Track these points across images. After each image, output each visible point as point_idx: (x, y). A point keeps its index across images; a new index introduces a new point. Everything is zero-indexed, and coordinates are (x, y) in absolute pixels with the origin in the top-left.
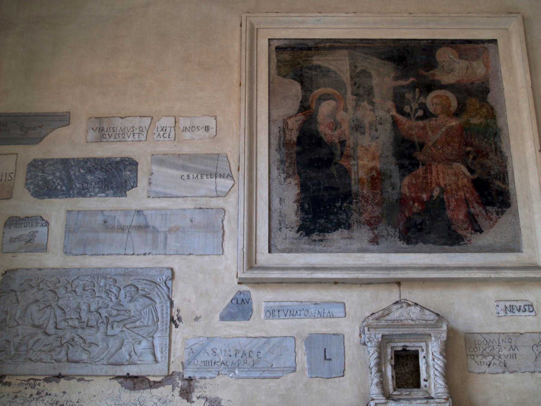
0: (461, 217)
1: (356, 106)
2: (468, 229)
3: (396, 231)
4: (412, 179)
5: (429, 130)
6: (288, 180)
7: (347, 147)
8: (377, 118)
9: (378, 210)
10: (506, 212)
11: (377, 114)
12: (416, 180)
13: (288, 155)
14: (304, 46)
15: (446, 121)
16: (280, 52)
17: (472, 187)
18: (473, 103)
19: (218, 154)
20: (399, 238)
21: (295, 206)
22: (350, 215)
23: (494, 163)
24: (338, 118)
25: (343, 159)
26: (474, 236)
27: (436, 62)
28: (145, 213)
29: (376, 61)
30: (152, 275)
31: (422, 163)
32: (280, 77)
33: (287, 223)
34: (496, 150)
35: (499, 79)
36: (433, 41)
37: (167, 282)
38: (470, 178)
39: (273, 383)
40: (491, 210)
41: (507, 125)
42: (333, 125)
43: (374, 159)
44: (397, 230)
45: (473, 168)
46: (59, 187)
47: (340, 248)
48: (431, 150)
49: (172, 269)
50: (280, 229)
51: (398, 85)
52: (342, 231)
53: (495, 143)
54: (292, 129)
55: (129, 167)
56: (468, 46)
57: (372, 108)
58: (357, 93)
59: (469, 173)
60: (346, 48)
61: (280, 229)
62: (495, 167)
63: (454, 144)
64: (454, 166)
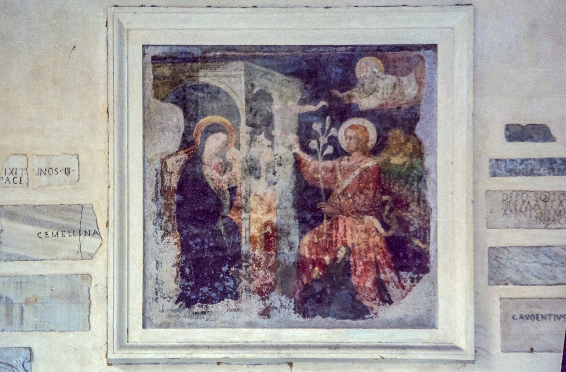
0: (369, 284)
1: (251, 141)
2: (375, 299)
3: (291, 302)
4: (313, 237)
5: (339, 173)
6: (167, 239)
7: (238, 195)
8: (277, 157)
9: (272, 276)
10: (423, 278)
11: (276, 152)
12: (318, 238)
13: (167, 207)
14: (188, 56)
15: (361, 161)
16: (157, 65)
17: (385, 247)
18: (397, 134)
19: (83, 206)
20: (294, 309)
21: (174, 271)
22: (238, 281)
23: (414, 217)
24: (229, 156)
25: (232, 212)
26: (382, 307)
27: (355, 79)
29: (279, 77)
30: (7, 357)
31: (327, 216)
32: (157, 101)
33: (164, 291)
34: (419, 200)
35: (433, 102)
36: (354, 48)
37: (25, 365)
38: (384, 235)
40: (404, 276)
42: (222, 166)
43: (269, 211)
44: (293, 300)
45: (388, 222)
47: (224, 322)
48: (340, 199)
49: (30, 349)
50: (157, 299)
51: (305, 111)
52: (228, 302)
53: (419, 190)
54: (172, 172)
56: (399, 54)
57: (270, 143)
58: (253, 123)
59: (382, 229)
60: (242, 59)
61: (157, 299)
62: (416, 221)
63: (368, 192)
64: (366, 220)
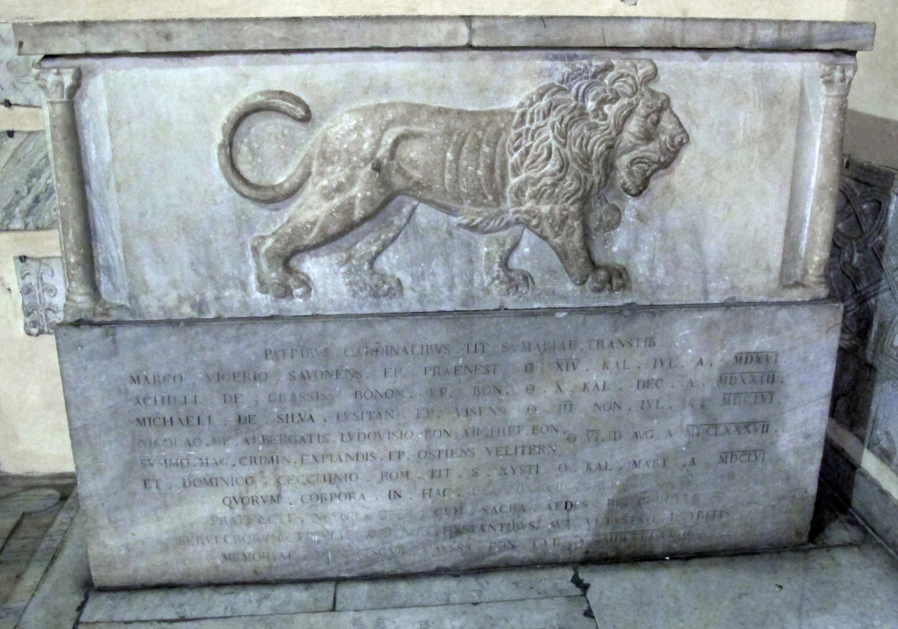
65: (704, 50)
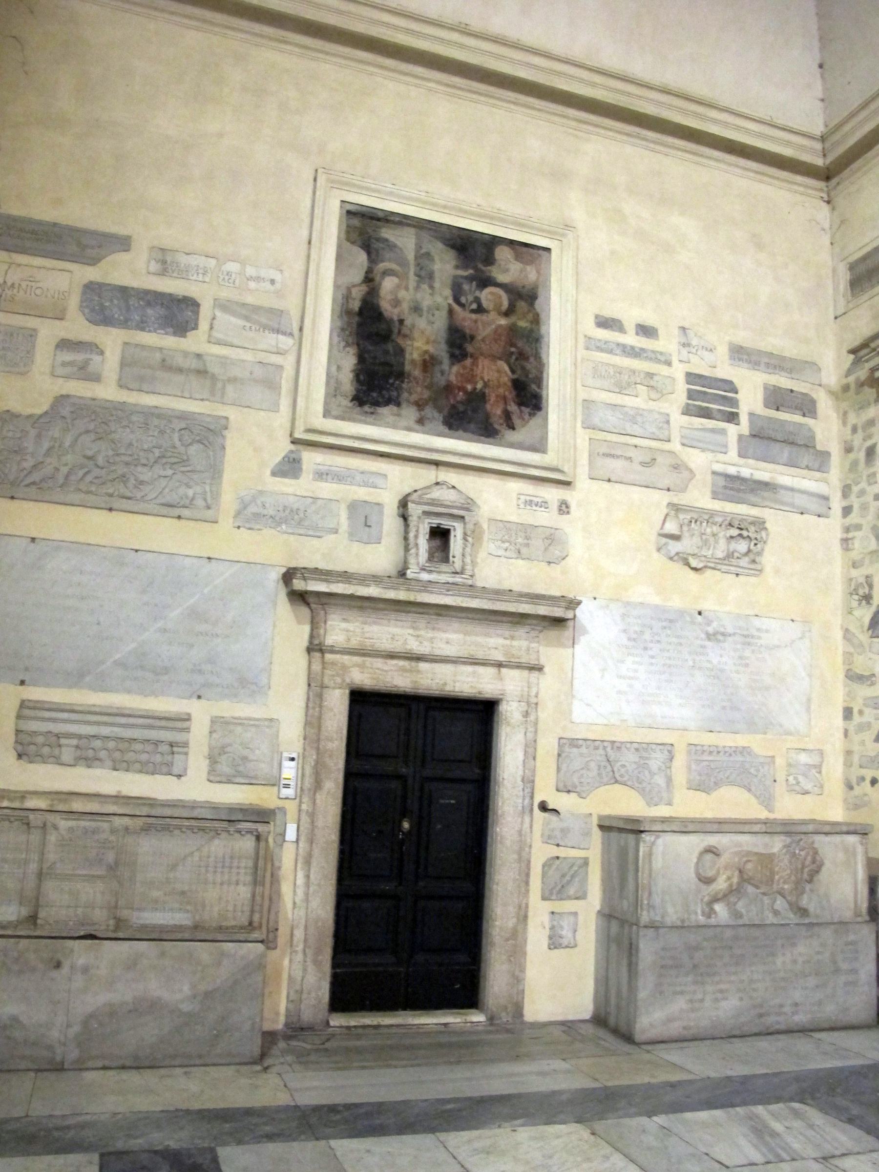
6: (348, 349)
13: (349, 324)
18: (522, 305)
19: (282, 311)
21: (351, 376)
27: (495, 260)
28: (205, 357)
29: (440, 245)
35: (548, 289)
39: (315, 541)
41: (549, 333)
43: (427, 343)
45: (514, 368)
46: (116, 316)
53: (536, 349)
55: (191, 308)
56: (525, 249)
60: (414, 226)
65: (826, 834)
